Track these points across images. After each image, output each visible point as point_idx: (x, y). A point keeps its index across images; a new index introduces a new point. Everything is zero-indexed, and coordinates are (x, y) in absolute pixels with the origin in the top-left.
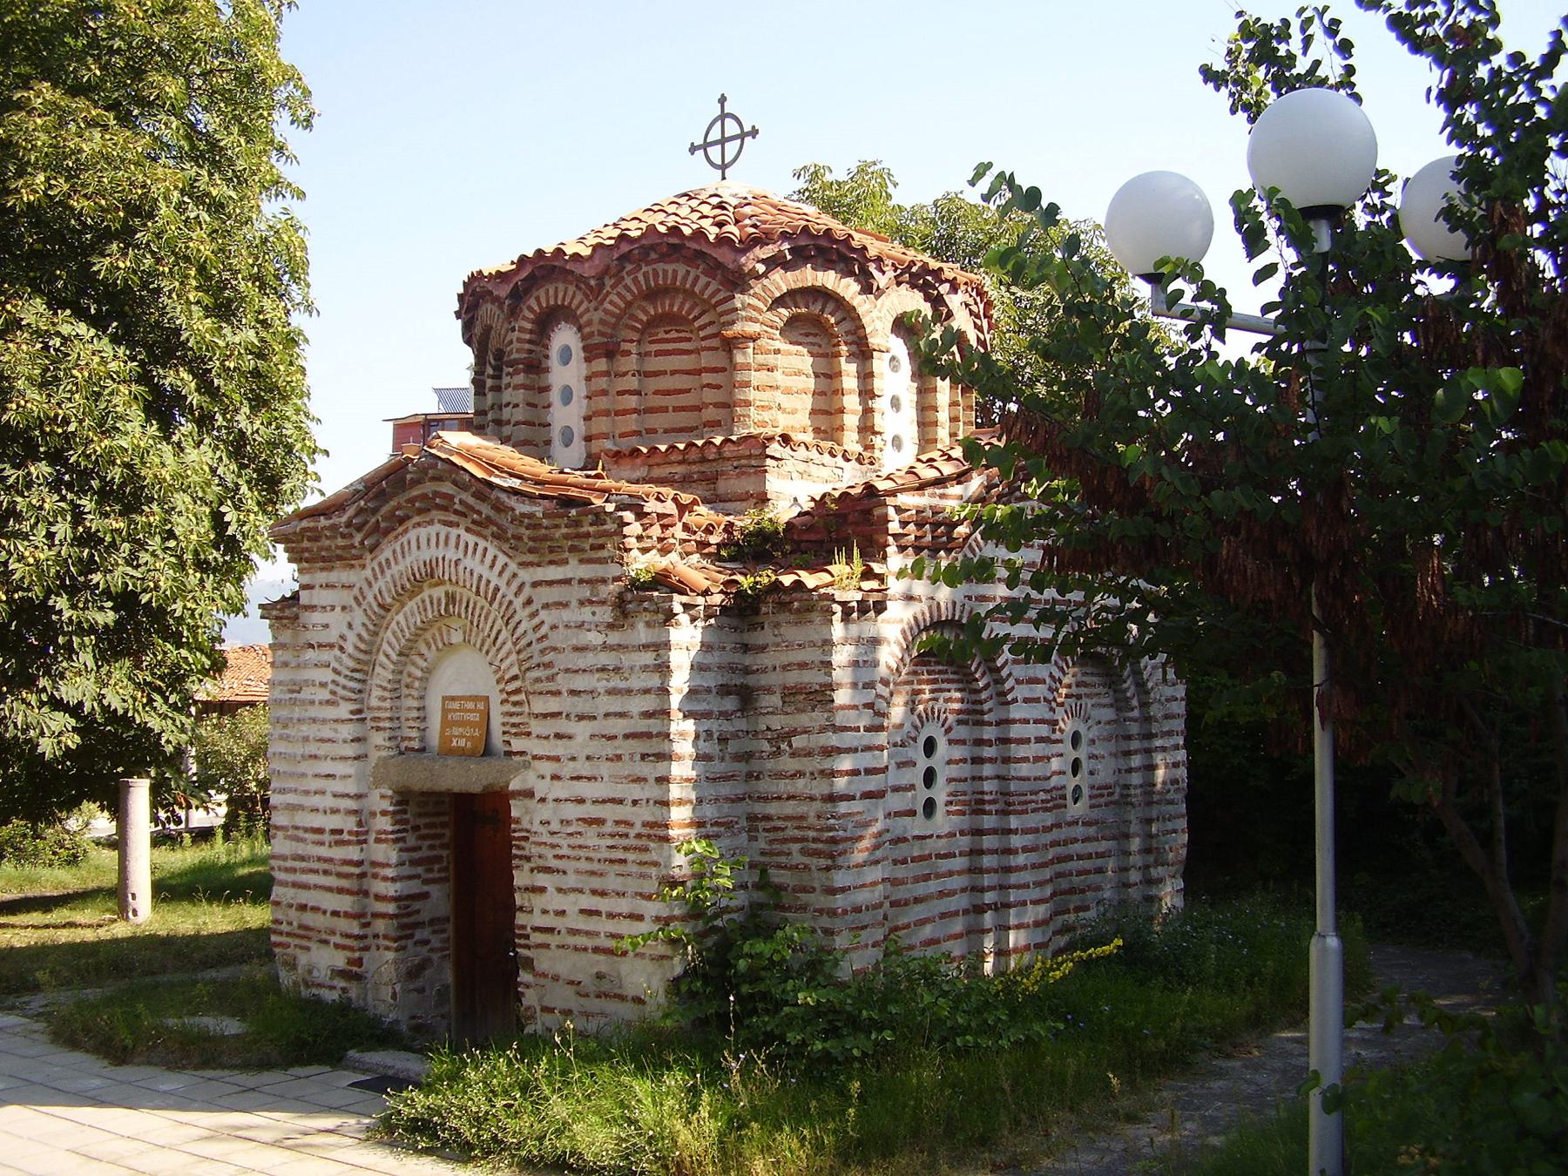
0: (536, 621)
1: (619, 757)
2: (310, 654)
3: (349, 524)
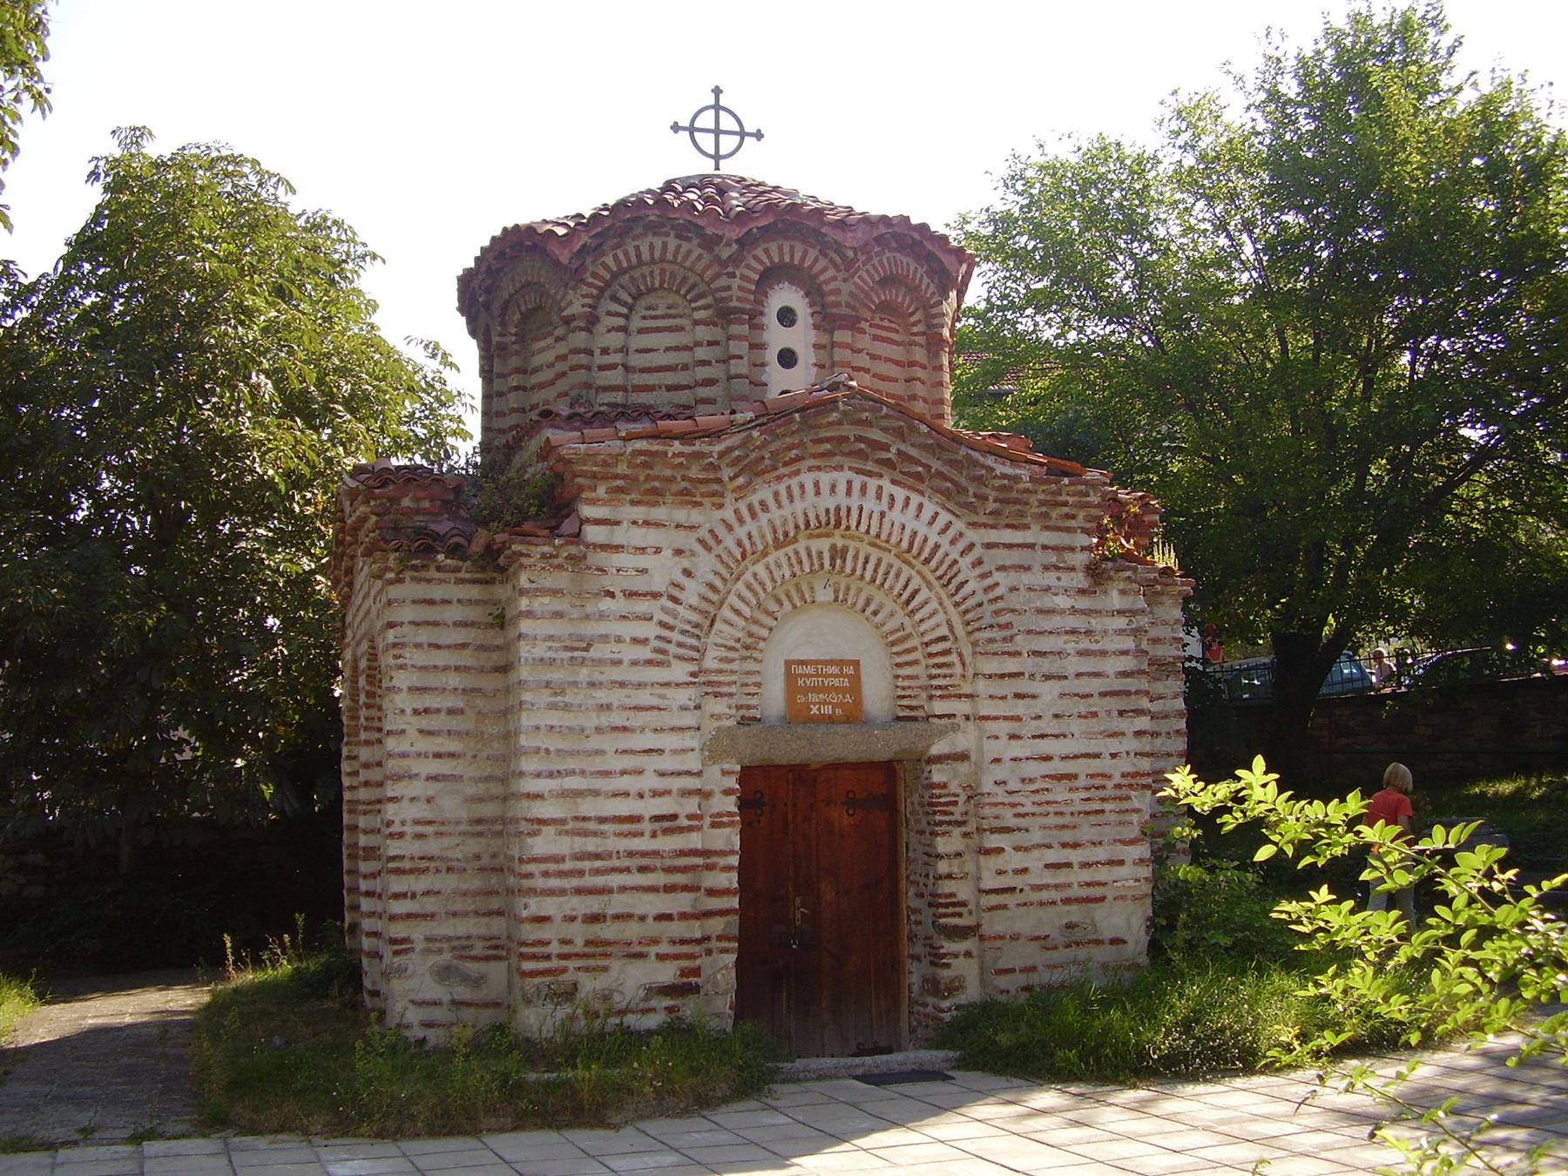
0: (988, 582)
1: (1094, 714)
2: (606, 604)
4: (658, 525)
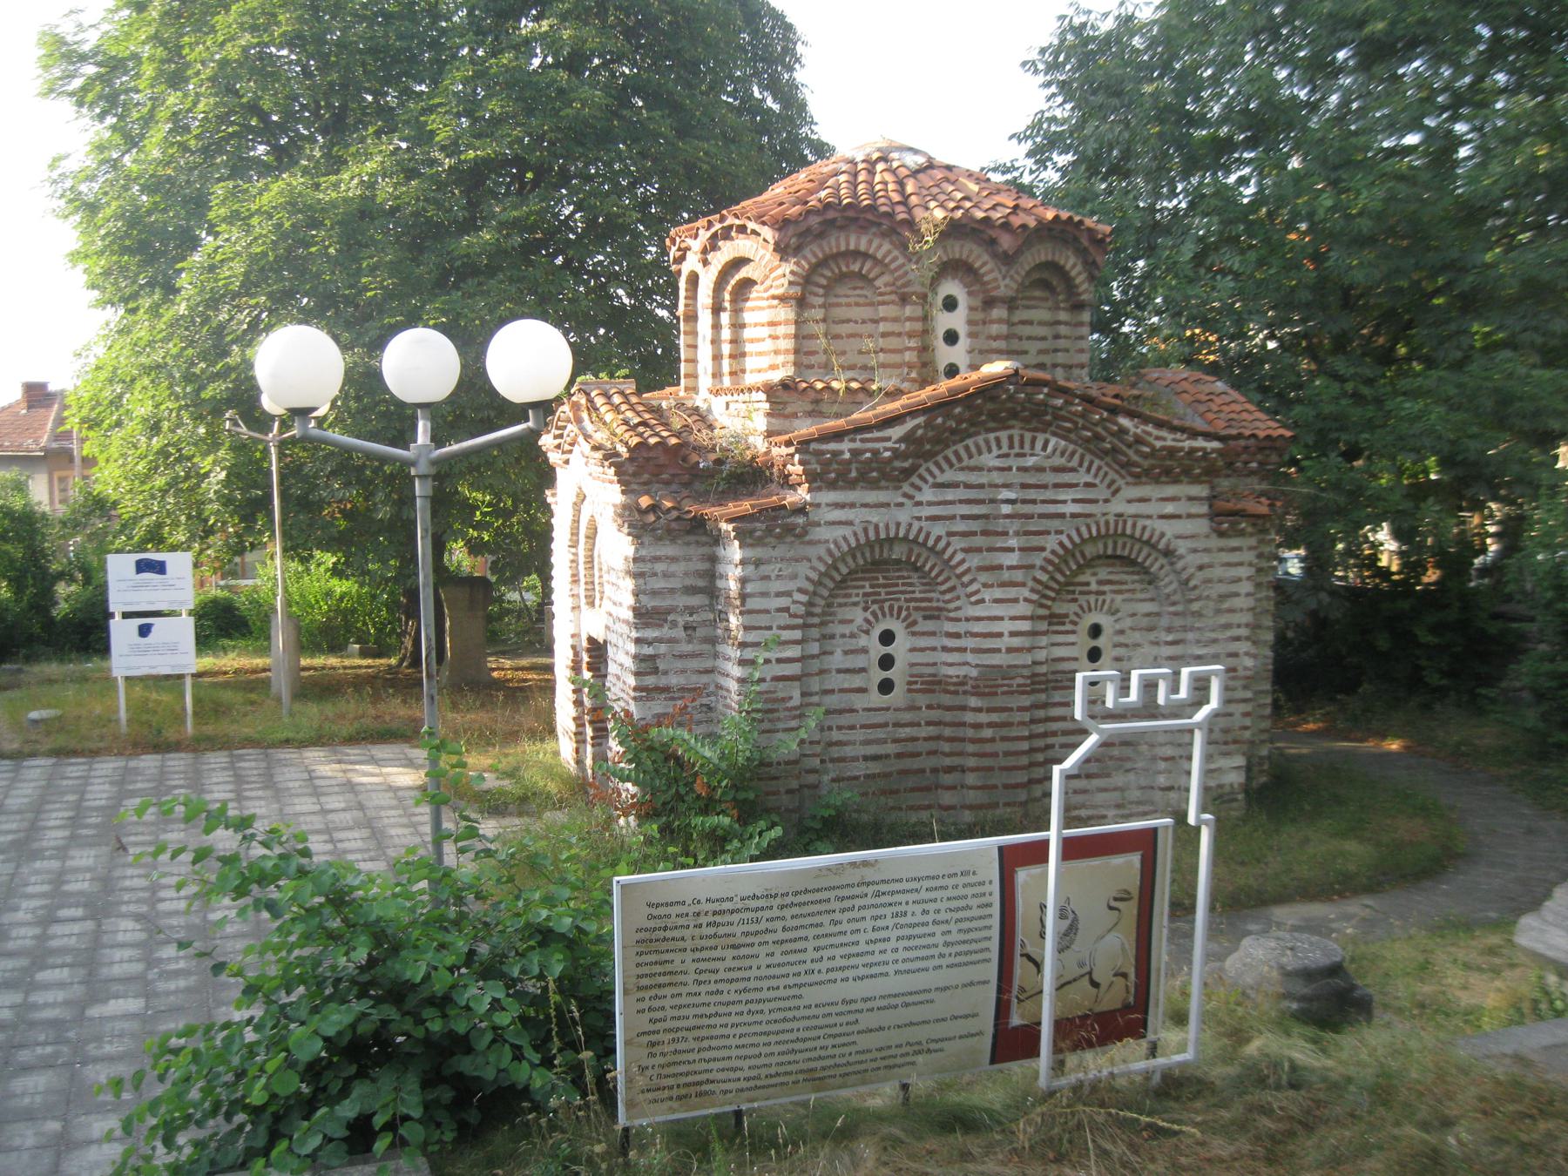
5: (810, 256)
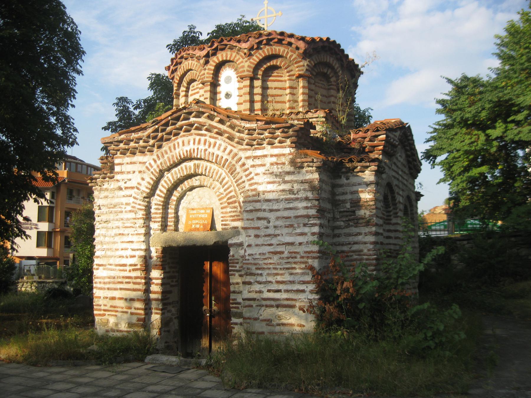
3: (149, 137)
4: (134, 163)
5: (315, 60)
